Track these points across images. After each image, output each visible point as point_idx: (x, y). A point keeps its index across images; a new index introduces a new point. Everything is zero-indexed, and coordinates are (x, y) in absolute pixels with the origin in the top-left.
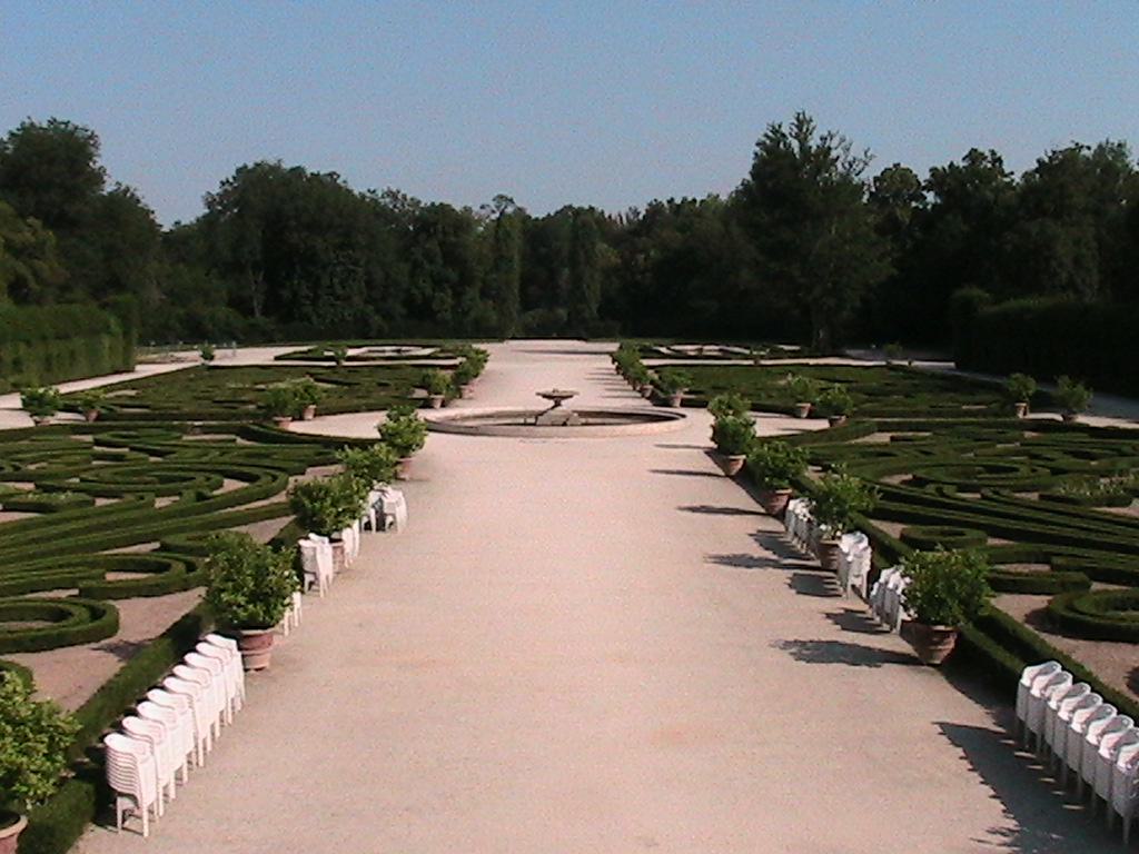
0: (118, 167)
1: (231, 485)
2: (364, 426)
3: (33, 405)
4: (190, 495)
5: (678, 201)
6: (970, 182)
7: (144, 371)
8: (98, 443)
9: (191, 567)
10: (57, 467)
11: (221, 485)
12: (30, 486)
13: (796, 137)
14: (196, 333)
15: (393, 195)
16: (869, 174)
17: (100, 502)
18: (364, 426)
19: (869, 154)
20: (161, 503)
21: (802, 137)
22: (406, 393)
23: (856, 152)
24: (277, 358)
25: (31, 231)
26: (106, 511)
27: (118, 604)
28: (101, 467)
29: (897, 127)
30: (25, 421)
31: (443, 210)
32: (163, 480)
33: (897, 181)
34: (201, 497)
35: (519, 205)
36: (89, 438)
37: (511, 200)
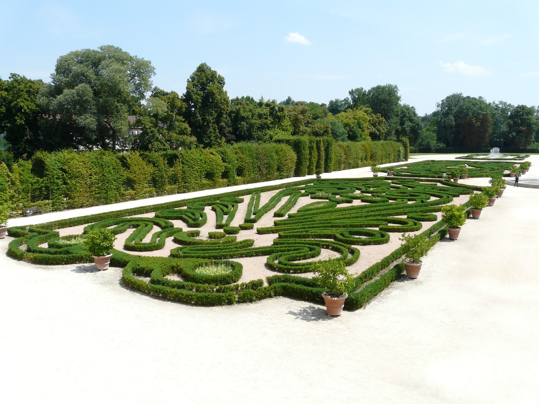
1: (433, 199)
4: (419, 201)
7: (410, 161)
14: (426, 150)
20: (410, 203)
24: (456, 158)
26: (391, 204)
27: (390, 234)
34: (422, 202)
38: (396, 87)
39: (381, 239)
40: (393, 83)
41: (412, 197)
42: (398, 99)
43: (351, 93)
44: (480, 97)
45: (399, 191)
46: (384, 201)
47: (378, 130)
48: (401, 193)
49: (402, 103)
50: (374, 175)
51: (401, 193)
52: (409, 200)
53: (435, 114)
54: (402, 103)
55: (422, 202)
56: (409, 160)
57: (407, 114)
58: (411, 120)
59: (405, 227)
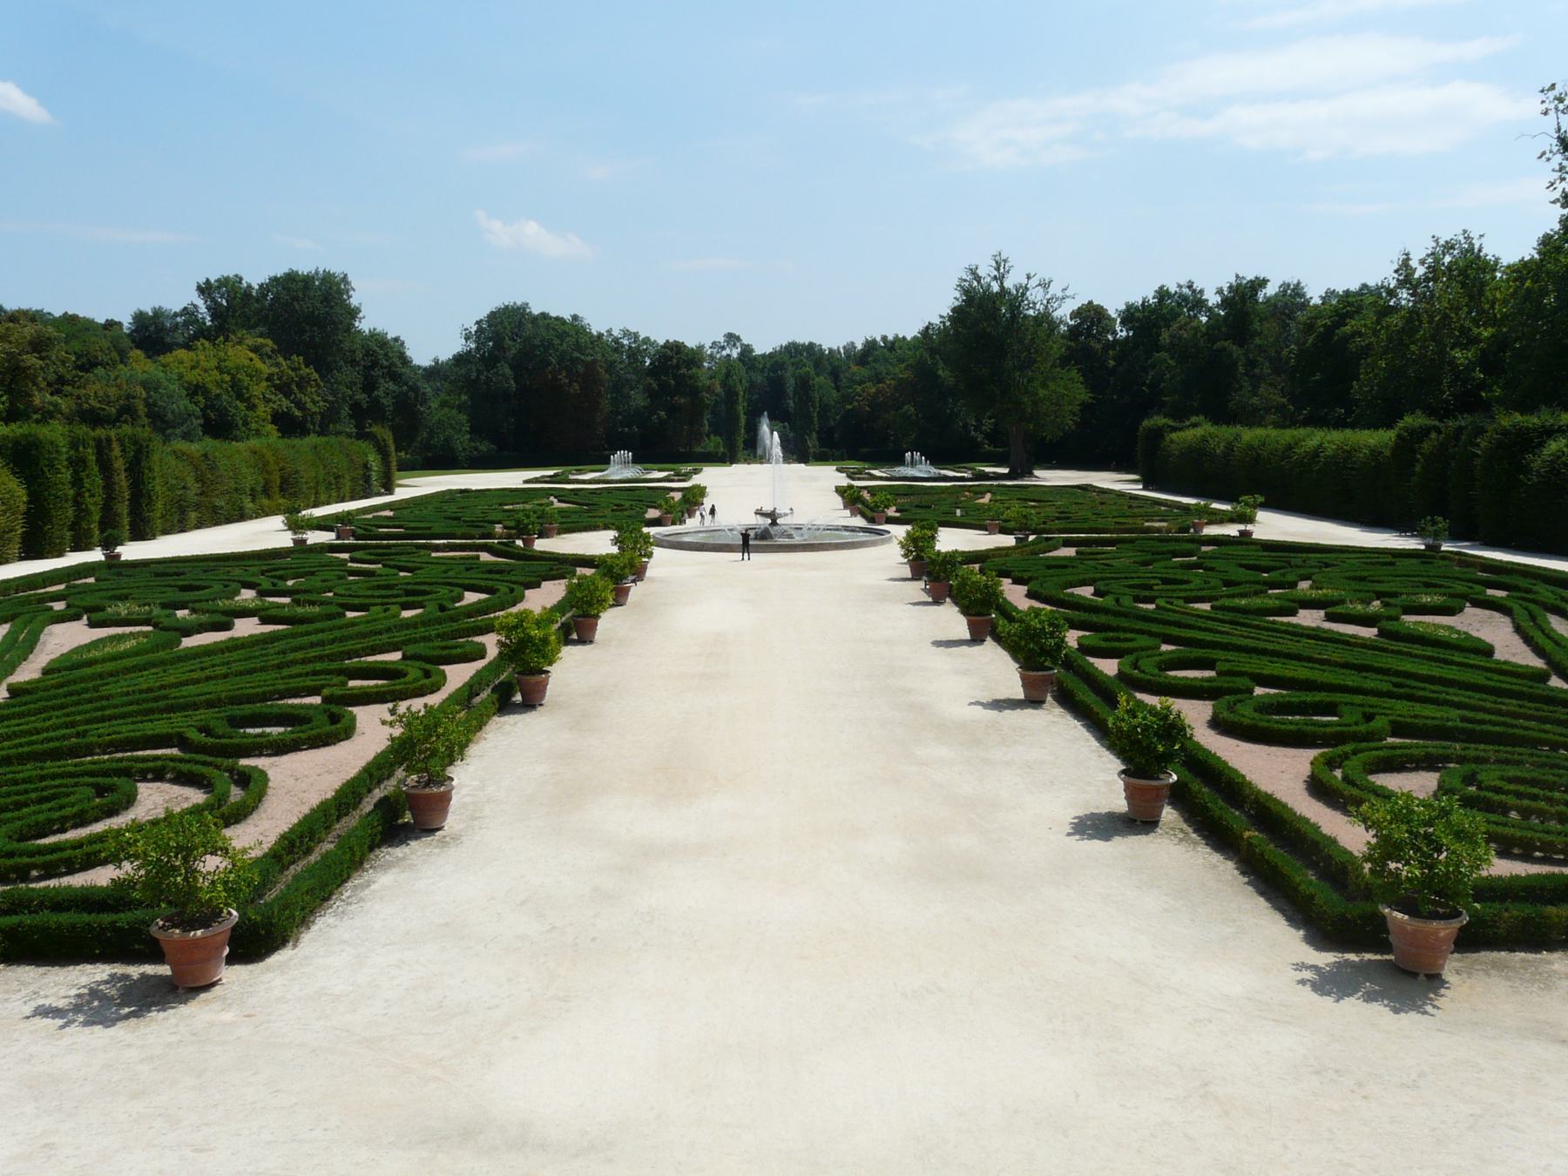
0: (377, 311)
1: (471, 598)
2: (600, 543)
3: (295, 526)
4: (432, 608)
5: (890, 338)
6: (1159, 318)
7: (400, 494)
8: (353, 560)
9: (427, 674)
10: (315, 582)
11: (461, 598)
12: (287, 600)
13: (995, 278)
15: (626, 333)
16: (1064, 312)
17: (350, 614)
18: (600, 543)
19: (1068, 293)
20: (407, 614)
21: (1000, 279)
22: (627, 513)
23: (1055, 290)
24: (526, 482)
25: (291, 366)
26: (353, 623)
27: (355, 710)
28: (356, 582)
29: (1094, 267)
30: (285, 540)
31: (675, 348)
32: (408, 593)
33: (1091, 315)
34: (442, 608)
35: (745, 342)
36: (346, 556)
37: (738, 338)
38: (345, 279)
39: (329, 728)
40: (336, 268)
41: (412, 596)
42: (353, 313)
43: (205, 289)
44: (575, 317)
45: (374, 581)
46: (330, 617)
47: (300, 405)
48: (379, 587)
49: (365, 325)
50: (295, 541)
51: (379, 587)
52: (406, 606)
53: (459, 359)
54: (365, 325)
55: (442, 608)
56: (397, 490)
57: (383, 356)
58: (395, 377)
59: (398, 685)
